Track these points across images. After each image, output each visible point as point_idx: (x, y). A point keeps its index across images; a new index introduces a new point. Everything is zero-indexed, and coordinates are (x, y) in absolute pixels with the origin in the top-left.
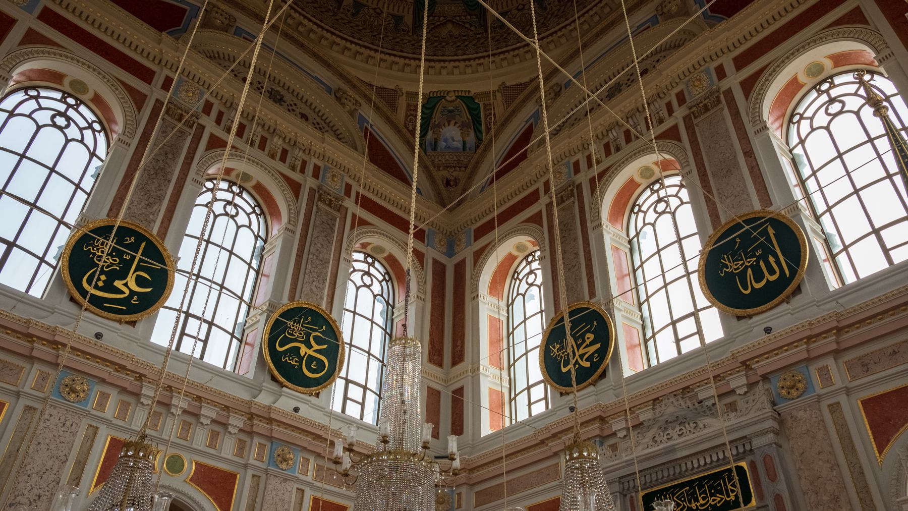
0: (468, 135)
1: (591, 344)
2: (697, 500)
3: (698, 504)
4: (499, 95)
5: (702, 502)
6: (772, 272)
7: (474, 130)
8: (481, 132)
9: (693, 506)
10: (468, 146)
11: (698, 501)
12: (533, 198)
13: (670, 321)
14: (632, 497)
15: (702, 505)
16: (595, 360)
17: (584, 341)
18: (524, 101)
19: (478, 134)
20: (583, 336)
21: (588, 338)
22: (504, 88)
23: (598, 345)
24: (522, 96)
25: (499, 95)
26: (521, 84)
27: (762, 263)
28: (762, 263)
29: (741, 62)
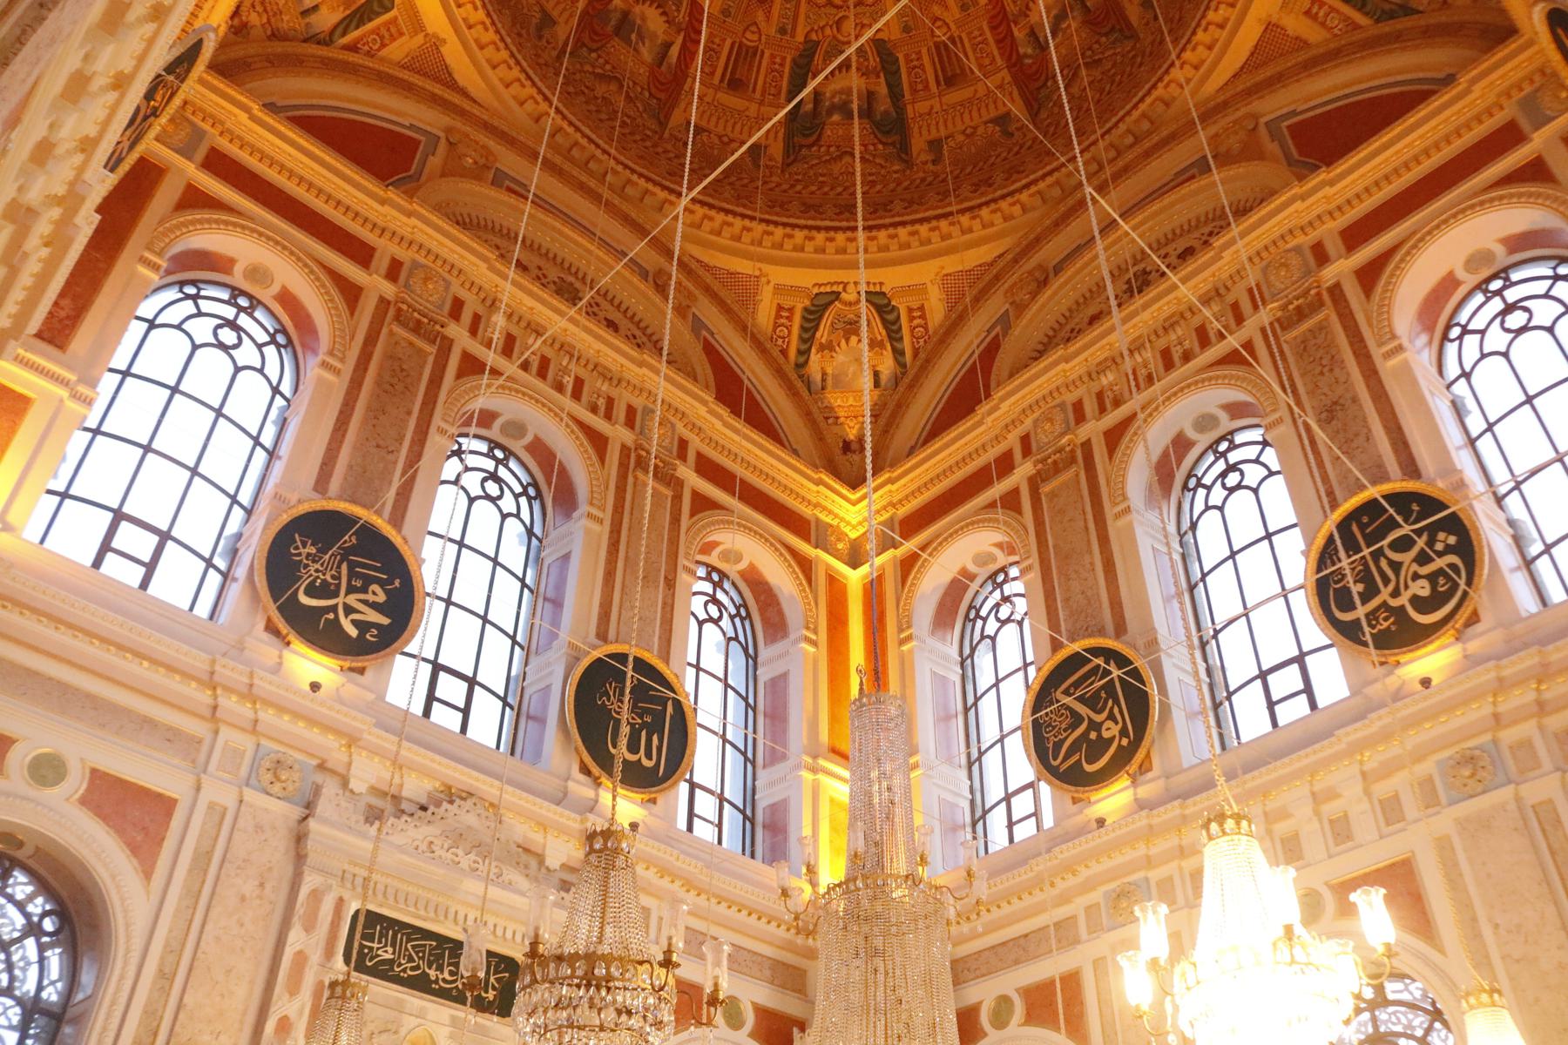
0: (333, 9)
1: (374, 606)
2: (440, 969)
3: (441, 977)
4: (420, 39)
5: (446, 976)
6: (649, 756)
7: (344, 19)
8: (344, 34)
9: (432, 973)
10: (313, 18)
11: (442, 972)
12: (362, 254)
13: (479, 679)
14: (341, 900)
15: (444, 980)
16: (368, 636)
17: (364, 590)
18: (435, 100)
19: (342, 26)
20: (368, 581)
21: (374, 593)
22: (435, 44)
23: (385, 621)
24: (437, 89)
25: (420, 39)
26: (450, 75)
27: (644, 733)
28: (644, 733)
29: (707, 469)
